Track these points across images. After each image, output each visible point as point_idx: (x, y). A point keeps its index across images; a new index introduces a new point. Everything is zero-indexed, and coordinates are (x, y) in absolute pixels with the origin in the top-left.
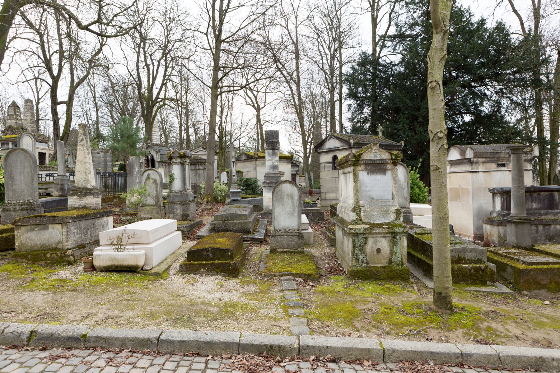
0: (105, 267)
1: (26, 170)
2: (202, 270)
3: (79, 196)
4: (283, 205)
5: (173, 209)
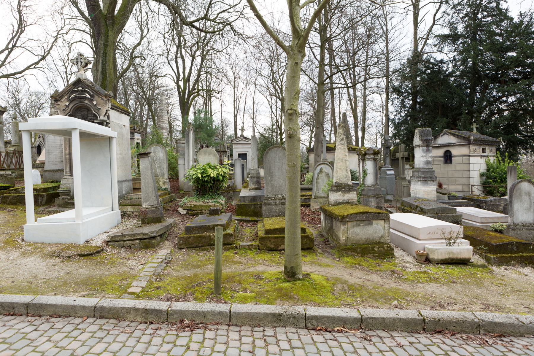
0: (442, 260)
1: (284, 167)
2: (513, 262)
3: (343, 191)
4: (521, 201)
5: (368, 202)
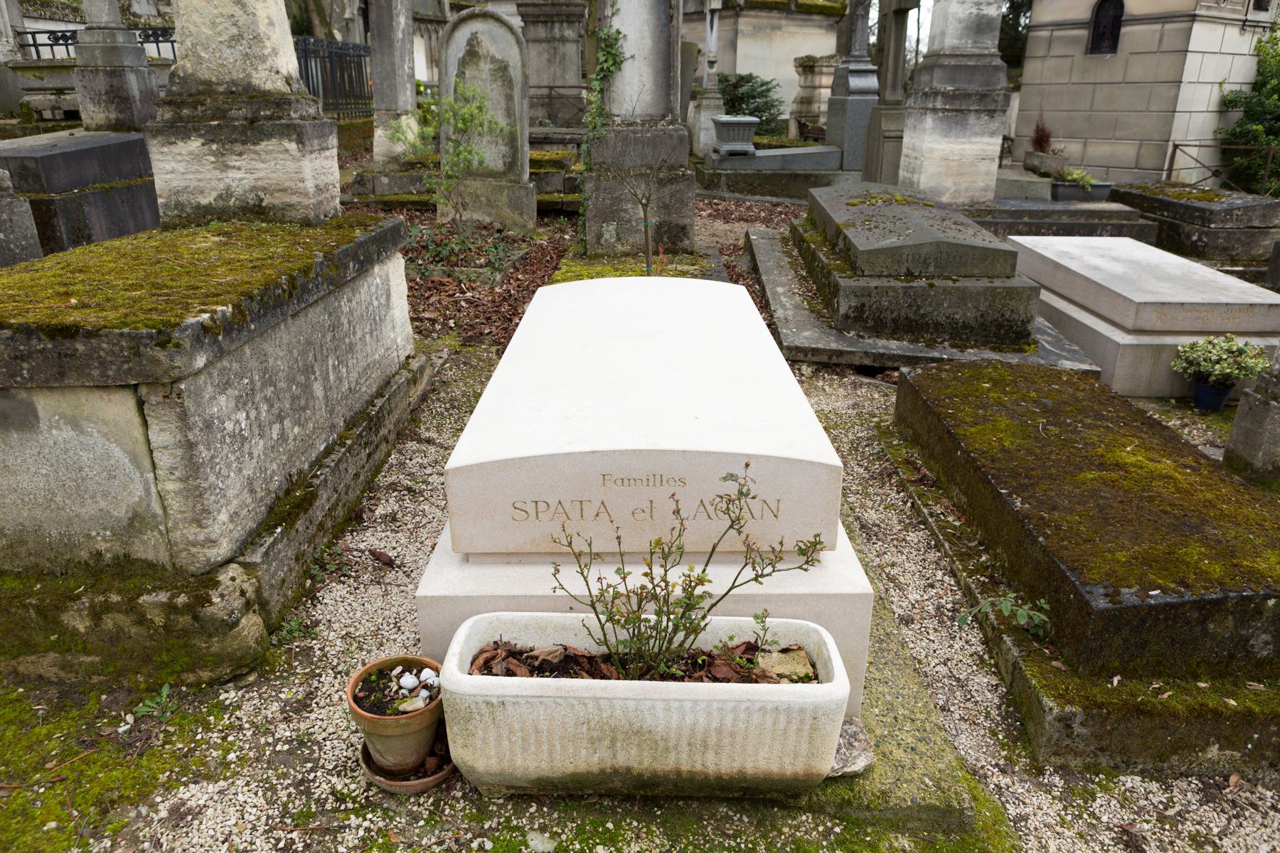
2: (1213, 752)
3: (211, 137)
